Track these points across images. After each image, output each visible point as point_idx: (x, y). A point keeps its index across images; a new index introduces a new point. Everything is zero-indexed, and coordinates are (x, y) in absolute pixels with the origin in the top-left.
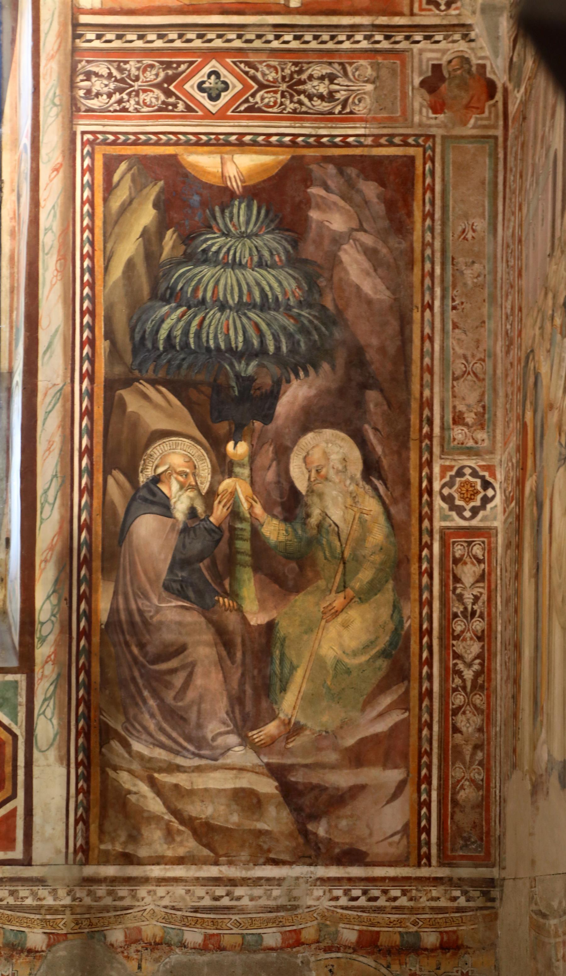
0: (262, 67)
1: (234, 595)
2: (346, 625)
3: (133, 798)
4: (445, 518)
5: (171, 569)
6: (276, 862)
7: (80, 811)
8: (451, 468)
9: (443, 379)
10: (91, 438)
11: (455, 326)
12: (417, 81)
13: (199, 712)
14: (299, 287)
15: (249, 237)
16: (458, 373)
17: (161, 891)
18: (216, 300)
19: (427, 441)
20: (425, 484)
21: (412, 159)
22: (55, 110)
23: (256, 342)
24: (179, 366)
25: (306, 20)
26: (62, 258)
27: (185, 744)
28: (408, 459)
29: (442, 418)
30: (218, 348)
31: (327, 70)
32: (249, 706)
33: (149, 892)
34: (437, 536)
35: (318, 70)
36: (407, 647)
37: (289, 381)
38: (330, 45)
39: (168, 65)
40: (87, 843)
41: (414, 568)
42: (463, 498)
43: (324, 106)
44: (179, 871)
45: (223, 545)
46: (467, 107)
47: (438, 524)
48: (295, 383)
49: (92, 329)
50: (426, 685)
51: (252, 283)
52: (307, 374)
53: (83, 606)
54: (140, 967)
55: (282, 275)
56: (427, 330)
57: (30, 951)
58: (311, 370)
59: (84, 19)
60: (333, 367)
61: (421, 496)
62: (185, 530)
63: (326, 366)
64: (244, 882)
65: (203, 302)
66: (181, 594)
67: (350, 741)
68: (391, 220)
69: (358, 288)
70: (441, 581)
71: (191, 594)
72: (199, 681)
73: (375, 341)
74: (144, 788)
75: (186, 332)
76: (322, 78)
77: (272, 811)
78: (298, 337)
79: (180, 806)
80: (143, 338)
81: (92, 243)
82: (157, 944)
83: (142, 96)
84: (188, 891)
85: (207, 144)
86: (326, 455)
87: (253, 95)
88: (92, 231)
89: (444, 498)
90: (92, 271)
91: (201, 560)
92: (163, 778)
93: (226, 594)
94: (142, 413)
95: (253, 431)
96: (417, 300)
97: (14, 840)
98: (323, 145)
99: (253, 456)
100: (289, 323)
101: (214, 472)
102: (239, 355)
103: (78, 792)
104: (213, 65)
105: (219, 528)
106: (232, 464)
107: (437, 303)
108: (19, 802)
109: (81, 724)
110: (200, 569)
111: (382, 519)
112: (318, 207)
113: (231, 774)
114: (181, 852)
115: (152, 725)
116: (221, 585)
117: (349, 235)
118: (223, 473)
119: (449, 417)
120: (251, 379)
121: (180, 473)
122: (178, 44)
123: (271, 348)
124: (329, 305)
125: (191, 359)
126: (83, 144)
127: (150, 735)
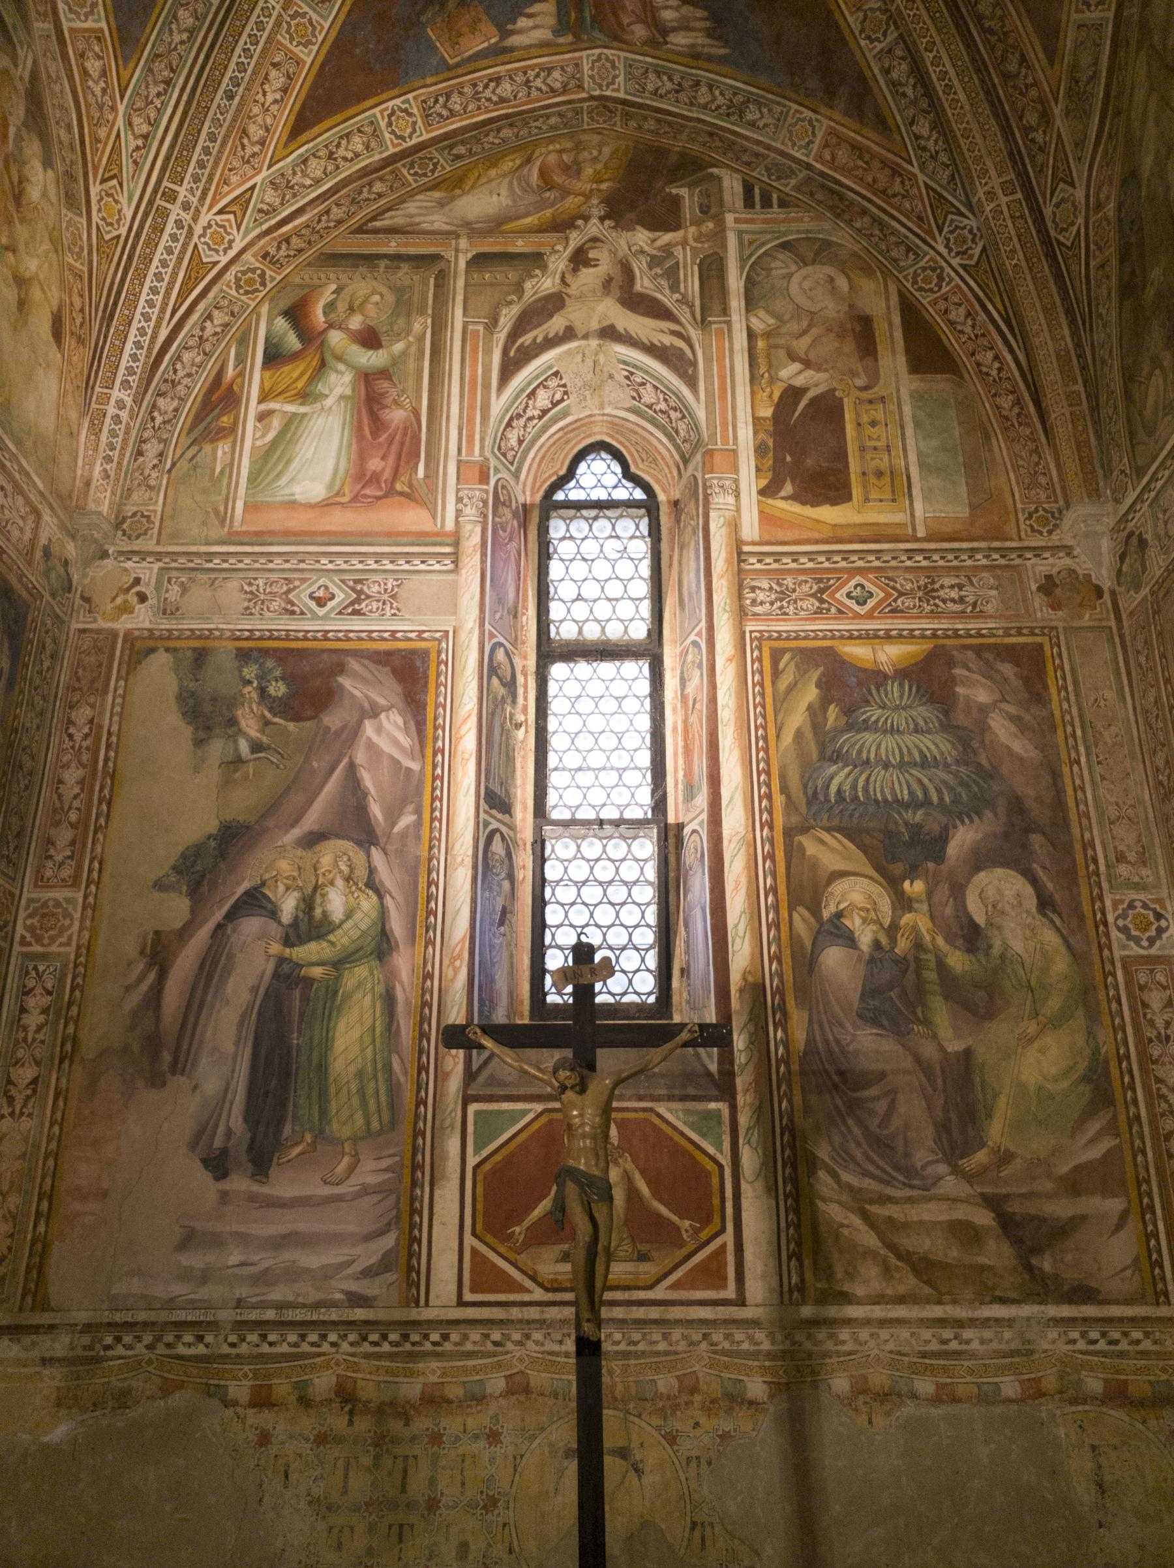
0: (900, 580)
1: (927, 1022)
2: (1042, 1051)
3: (845, 1232)
4: (1124, 947)
5: (863, 997)
6: (1003, 1301)
7: (792, 1246)
8: (1122, 901)
9: (1100, 823)
10: (774, 877)
11: (1103, 778)
12: (1034, 587)
13: (906, 1140)
14: (954, 747)
15: (904, 708)
16: (1113, 817)
17: (884, 1334)
18: (878, 760)
19: (1094, 878)
20: (1099, 916)
21: (1041, 646)
22: (726, 615)
23: (920, 794)
24: (851, 816)
25: (932, 546)
26: (738, 728)
27: (895, 1174)
28: (1079, 894)
29: (1106, 857)
30: (886, 800)
31: (955, 581)
32: (956, 1134)
33: (872, 1335)
34: (1118, 965)
35: (947, 581)
36: (1107, 1073)
37: (955, 827)
38: (955, 563)
39: (820, 580)
40: (803, 1280)
41: (1101, 995)
42: (1138, 929)
43: (958, 607)
44: (901, 1312)
45: (911, 975)
46: (1081, 605)
47: (1117, 954)
48: (961, 829)
49: (768, 785)
50: (1132, 1110)
51: (911, 746)
52: (971, 820)
53: (779, 1034)
54: (870, 1422)
55: (938, 739)
56: (1078, 782)
57: (751, 1403)
58: (976, 818)
59: (746, 549)
60: (996, 815)
61: (1097, 928)
62: (872, 961)
63: (988, 814)
64: (973, 1323)
65: (868, 761)
66: (875, 1022)
67: (1064, 1169)
68: (1030, 693)
69: (1009, 748)
70: (1130, 1007)
71: (886, 1023)
72: (902, 1109)
73: (1031, 793)
74: (857, 1221)
75: (854, 787)
76: (952, 587)
77: (991, 1244)
78: (959, 789)
79: (895, 1240)
80: (815, 792)
81: (764, 717)
82: (885, 1395)
83: (800, 604)
84: (913, 1334)
85: (859, 637)
86: (1000, 891)
87: (895, 600)
88: (764, 707)
89: (1119, 929)
90: (765, 739)
91: (892, 989)
92: (874, 1209)
93: (920, 1022)
94: (820, 856)
95: (927, 870)
96: (1064, 756)
97: (725, 1278)
98: (960, 636)
99: (929, 894)
100: (950, 778)
101: (894, 907)
102: (907, 806)
103: (788, 1227)
104: (858, 579)
105: (905, 959)
106: (910, 900)
107: (1083, 760)
108: (728, 1237)
109: (787, 1153)
110: (891, 999)
111: (1063, 949)
112: (963, 684)
113: (944, 1205)
114: (902, 1289)
115: (858, 1155)
116: (915, 1014)
117: (994, 706)
118: (903, 908)
119: (1111, 856)
120: (919, 826)
121: (861, 909)
122: (827, 565)
123: (935, 800)
124: (984, 762)
125: (861, 809)
126: (752, 641)
127: (858, 1164)
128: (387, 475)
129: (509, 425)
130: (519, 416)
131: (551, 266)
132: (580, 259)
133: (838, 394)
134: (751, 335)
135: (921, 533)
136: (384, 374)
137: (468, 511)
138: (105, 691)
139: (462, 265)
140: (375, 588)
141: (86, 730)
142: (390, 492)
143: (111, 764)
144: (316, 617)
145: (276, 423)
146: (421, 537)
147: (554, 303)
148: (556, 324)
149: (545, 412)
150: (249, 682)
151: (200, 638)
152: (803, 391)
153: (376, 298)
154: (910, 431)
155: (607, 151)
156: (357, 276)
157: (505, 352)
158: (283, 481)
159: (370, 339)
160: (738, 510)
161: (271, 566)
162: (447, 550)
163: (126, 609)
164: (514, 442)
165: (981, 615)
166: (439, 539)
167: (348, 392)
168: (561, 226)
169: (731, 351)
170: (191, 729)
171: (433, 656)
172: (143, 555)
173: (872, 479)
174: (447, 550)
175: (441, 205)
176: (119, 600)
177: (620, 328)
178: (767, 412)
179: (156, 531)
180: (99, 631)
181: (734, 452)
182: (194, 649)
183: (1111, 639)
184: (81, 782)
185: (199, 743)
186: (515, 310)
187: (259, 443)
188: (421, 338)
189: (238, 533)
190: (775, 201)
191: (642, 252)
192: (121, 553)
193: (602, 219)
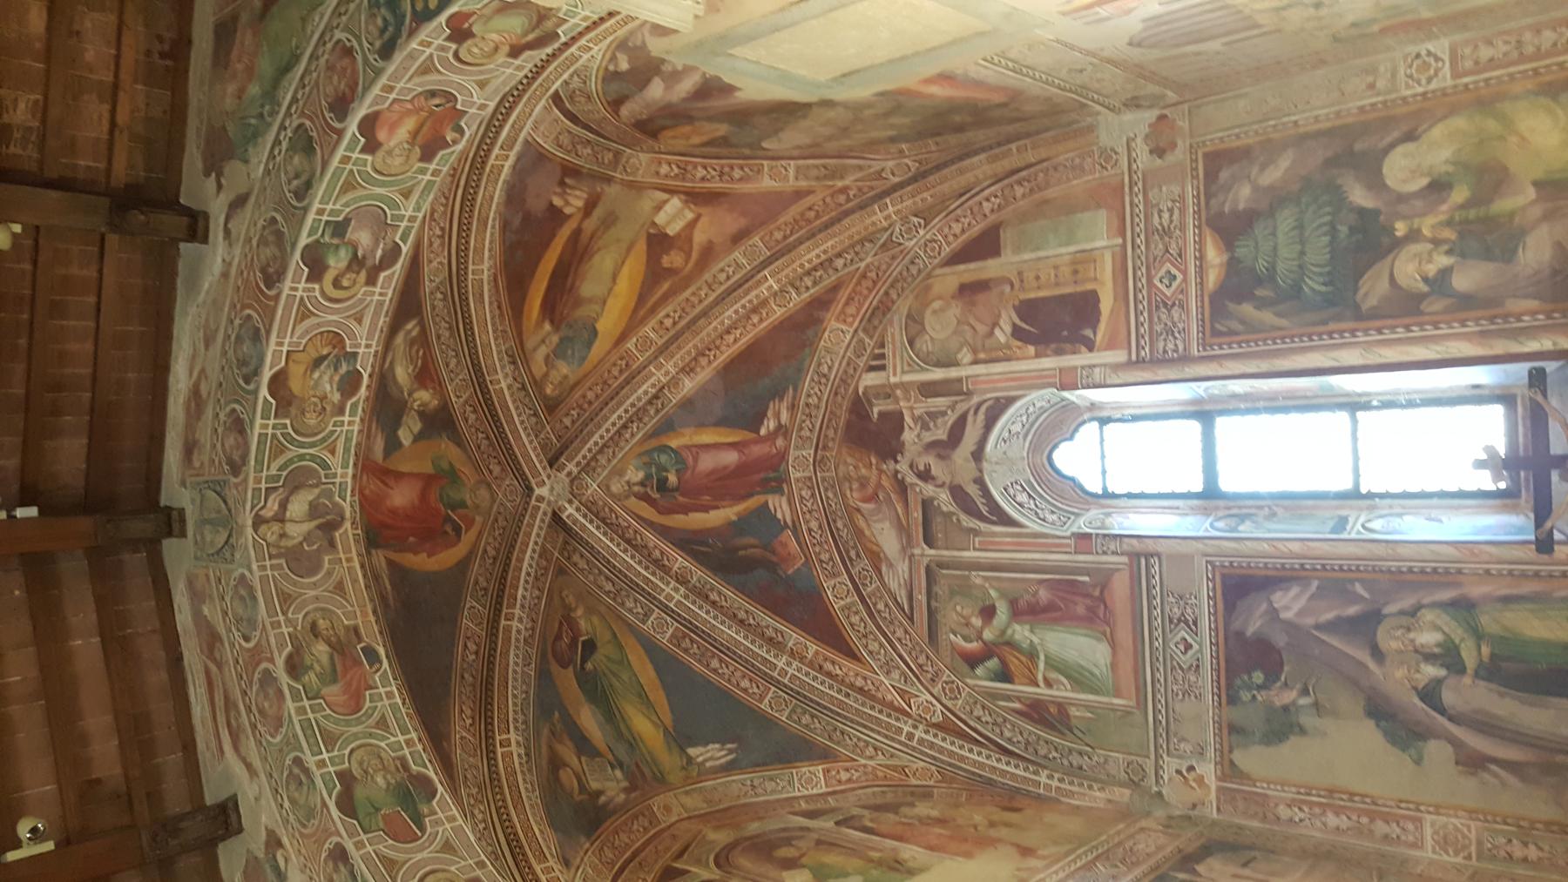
12: (1159, 161)
22: (1187, 369)
31: (1156, 215)
39: (1157, 307)
43: (1176, 212)
59: (1134, 357)
76: (1160, 217)
85: (1202, 278)
128: (1088, 601)
129: (1044, 520)
130: (1036, 513)
131: (931, 494)
132: (925, 476)
133: (1017, 303)
134: (975, 362)
135: (1120, 241)
136: (1013, 603)
137: (1112, 547)
138: (1266, 796)
139: (932, 552)
140: (1176, 610)
141: (1296, 810)
142: (1101, 599)
143: (1322, 793)
144: (1200, 650)
145: (1053, 675)
146: (1135, 579)
147: (957, 492)
148: (973, 490)
149: (1030, 496)
150: (1254, 697)
151: (1220, 730)
152: (1015, 326)
153: (958, 608)
154: (1042, 254)
155: (849, 460)
156: (944, 621)
157: (993, 523)
158: (1097, 672)
159: (988, 613)
160: (1105, 365)
161: (1162, 680)
162: (1143, 561)
163: (1200, 780)
164: (1054, 517)
165: (1182, 198)
166: (1135, 569)
167: (1028, 627)
168: (902, 488)
169: (988, 375)
170: (1292, 738)
171: (1225, 571)
172: (1158, 768)
173: (1080, 276)
174: (1143, 561)
175: (891, 565)
176: (1194, 784)
177: (973, 448)
178: (1031, 349)
179: (1139, 759)
180: (1218, 799)
181: (1060, 370)
182: (1230, 733)
183: (1198, 107)
184: (1337, 814)
185: (1303, 731)
186: (963, 517)
187: (1069, 687)
188: (986, 578)
189: (1138, 703)
190: (881, 351)
191: (918, 436)
192: (1157, 782)
193: (896, 461)
